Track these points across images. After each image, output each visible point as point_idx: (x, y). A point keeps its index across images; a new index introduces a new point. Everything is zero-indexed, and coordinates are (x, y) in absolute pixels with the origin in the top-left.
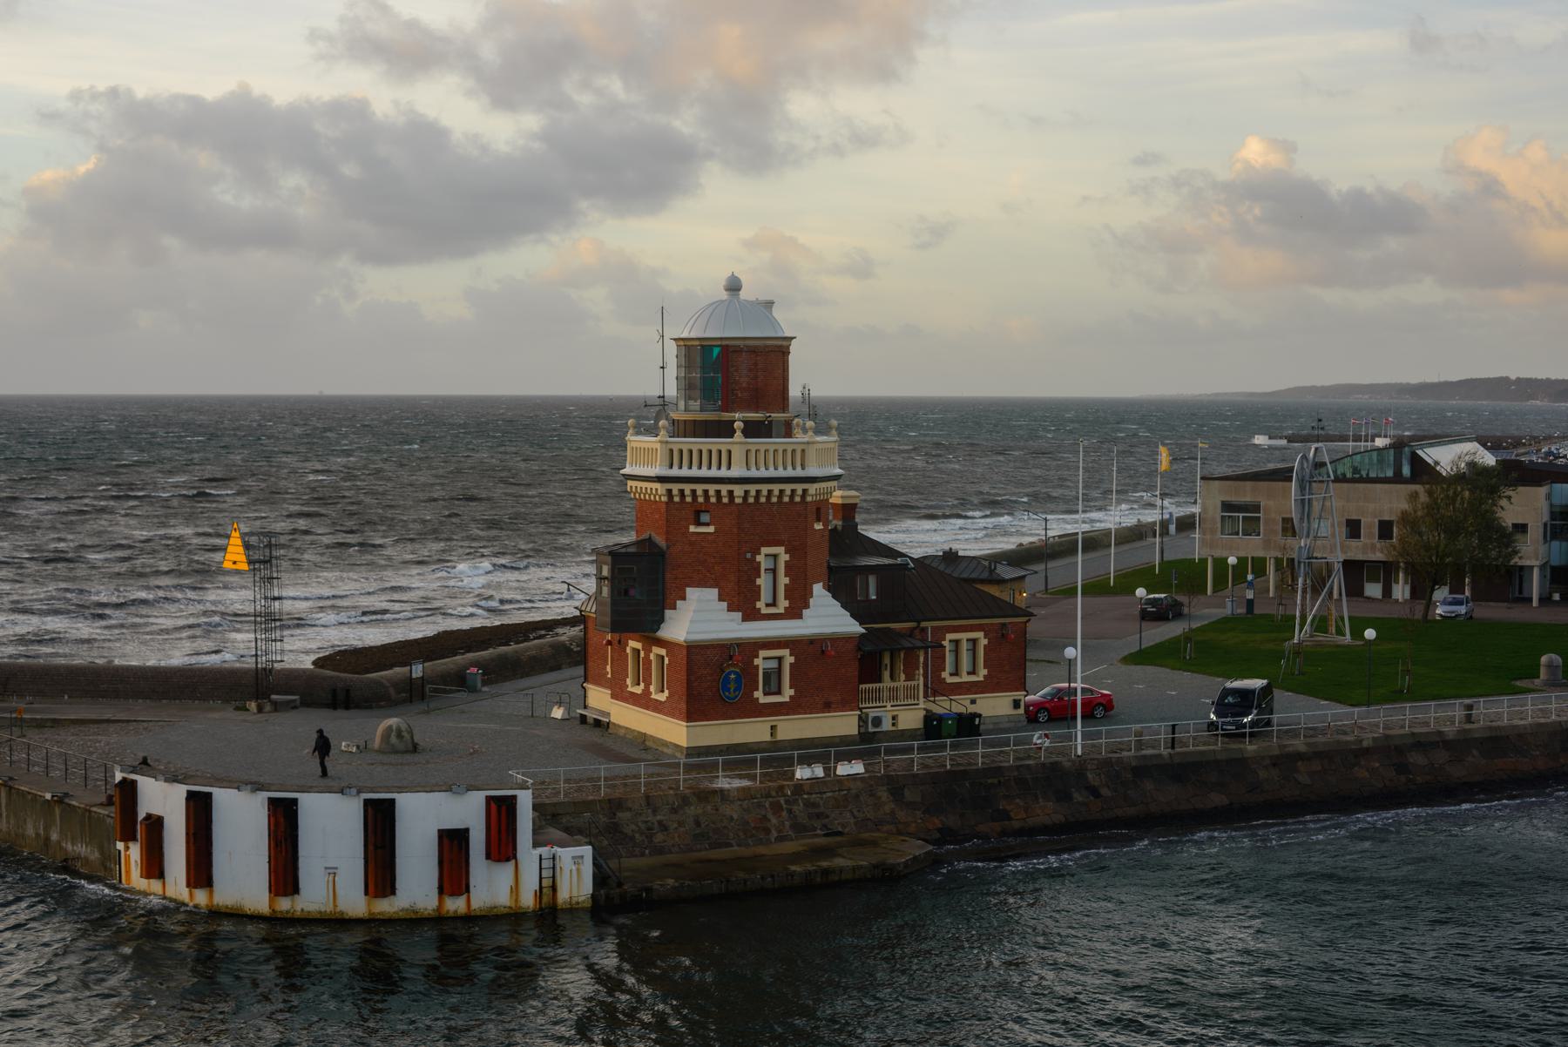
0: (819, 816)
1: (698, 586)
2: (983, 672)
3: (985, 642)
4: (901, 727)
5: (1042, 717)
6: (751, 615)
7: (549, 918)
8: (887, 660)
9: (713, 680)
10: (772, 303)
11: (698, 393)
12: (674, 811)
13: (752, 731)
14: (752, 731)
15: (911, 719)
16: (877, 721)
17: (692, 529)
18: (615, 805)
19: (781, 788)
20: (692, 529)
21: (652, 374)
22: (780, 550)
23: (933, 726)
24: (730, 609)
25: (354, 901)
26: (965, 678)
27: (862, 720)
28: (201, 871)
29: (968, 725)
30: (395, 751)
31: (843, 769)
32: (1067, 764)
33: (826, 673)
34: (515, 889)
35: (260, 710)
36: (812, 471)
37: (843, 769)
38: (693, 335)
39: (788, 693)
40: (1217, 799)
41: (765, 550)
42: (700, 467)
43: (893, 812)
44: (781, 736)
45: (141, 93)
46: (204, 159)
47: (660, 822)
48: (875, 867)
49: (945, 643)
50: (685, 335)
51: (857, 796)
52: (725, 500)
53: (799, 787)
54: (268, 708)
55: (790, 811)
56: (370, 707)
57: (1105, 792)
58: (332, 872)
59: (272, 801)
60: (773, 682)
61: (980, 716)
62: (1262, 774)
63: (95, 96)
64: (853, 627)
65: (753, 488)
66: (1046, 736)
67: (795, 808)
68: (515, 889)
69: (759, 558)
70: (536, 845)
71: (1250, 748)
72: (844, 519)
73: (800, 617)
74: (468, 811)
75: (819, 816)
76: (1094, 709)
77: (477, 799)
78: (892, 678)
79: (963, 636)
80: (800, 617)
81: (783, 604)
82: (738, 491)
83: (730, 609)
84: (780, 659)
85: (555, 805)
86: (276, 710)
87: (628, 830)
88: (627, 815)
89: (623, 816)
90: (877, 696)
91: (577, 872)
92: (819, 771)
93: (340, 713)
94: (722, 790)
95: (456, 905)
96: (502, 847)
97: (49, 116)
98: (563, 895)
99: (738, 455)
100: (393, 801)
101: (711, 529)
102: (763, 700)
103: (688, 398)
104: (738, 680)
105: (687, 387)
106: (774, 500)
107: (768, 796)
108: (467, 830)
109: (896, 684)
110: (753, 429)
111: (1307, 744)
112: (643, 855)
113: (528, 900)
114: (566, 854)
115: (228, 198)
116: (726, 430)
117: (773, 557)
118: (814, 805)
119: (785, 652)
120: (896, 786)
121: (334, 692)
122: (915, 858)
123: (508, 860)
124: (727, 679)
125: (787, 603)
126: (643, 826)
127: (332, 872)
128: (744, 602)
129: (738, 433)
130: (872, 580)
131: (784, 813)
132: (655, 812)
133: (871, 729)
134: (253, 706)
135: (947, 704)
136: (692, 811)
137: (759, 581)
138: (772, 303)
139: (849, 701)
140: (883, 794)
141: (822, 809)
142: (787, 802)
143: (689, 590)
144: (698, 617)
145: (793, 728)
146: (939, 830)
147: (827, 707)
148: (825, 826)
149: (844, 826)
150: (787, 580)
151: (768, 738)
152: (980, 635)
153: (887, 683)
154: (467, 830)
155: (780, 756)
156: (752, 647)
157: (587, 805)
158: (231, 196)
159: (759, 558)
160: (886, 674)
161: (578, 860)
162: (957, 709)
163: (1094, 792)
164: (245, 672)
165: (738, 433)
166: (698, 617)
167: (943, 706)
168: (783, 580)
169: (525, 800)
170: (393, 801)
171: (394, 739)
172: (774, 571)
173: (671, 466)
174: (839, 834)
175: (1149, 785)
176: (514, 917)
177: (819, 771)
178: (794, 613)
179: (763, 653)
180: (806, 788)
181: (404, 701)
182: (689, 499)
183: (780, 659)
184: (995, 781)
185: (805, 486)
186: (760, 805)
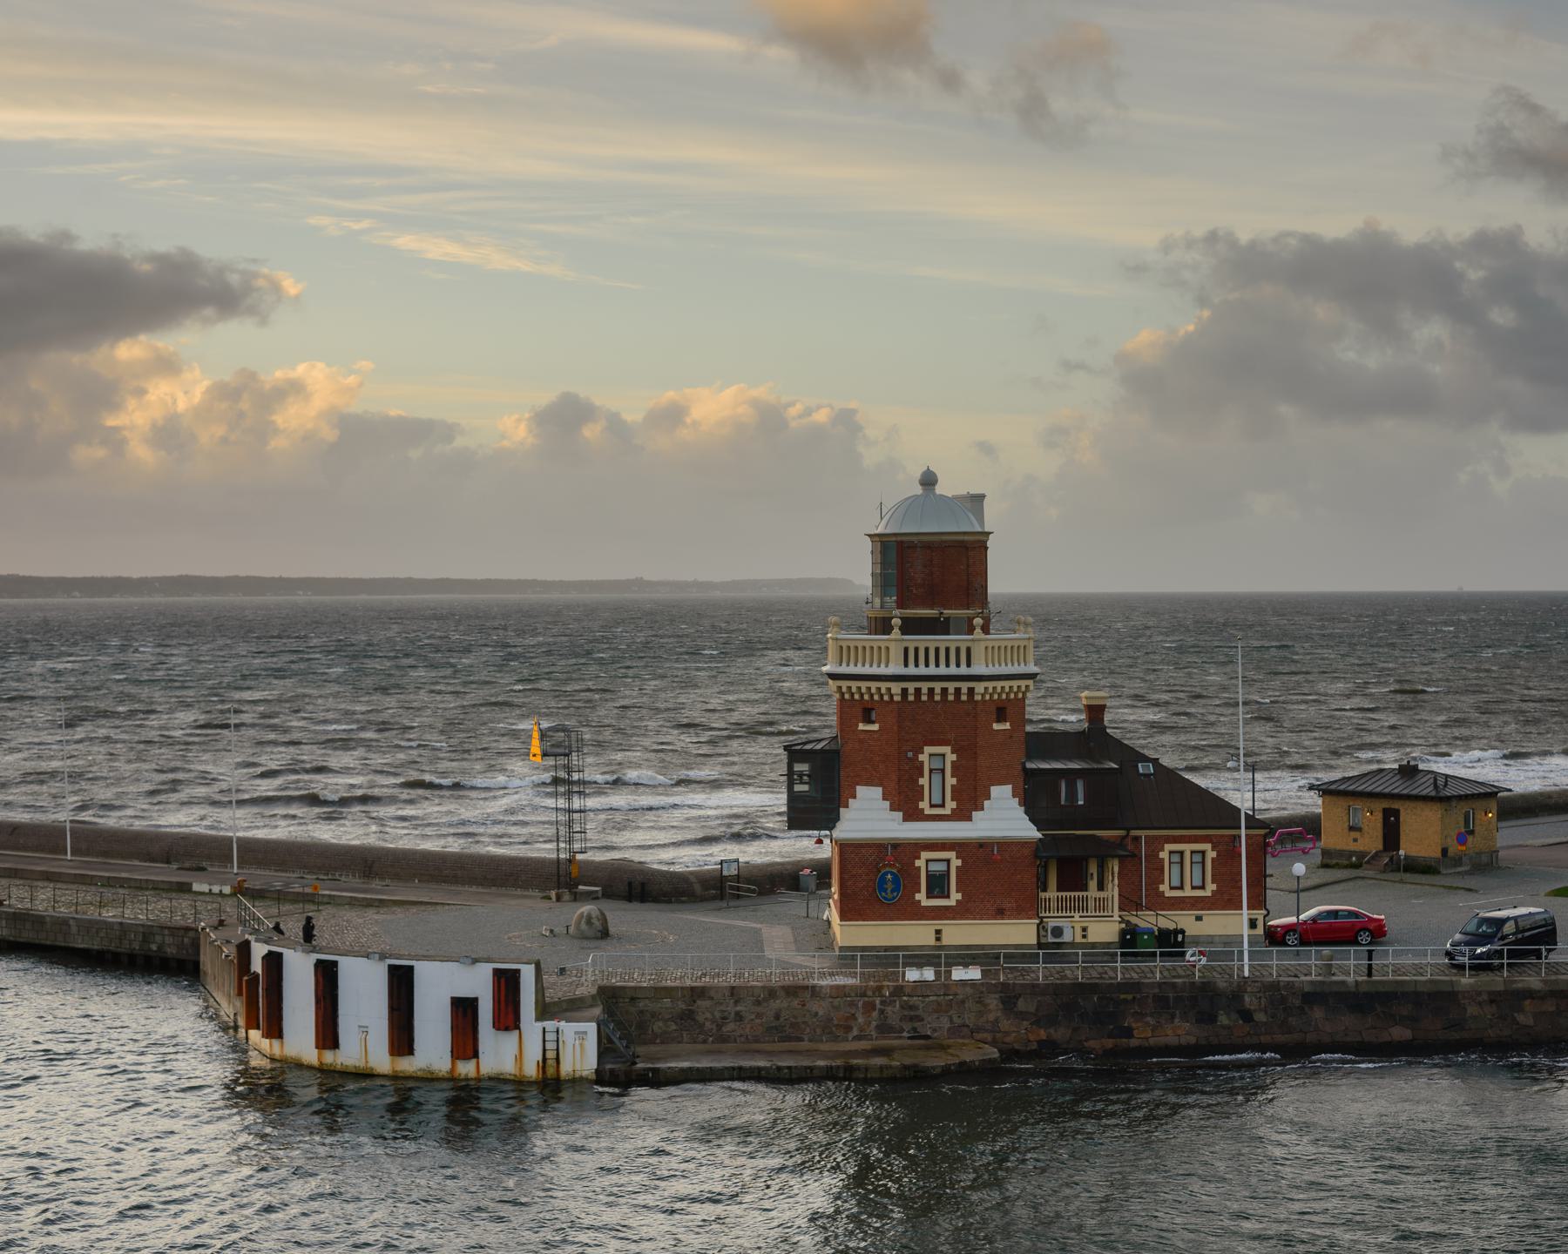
0: (911, 1019)
1: (867, 784)
2: (1211, 887)
3: (1214, 854)
4: (1091, 939)
5: (1291, 939)
6: (913, 815)
7: (551, 1087)
8: (1093, 869)
9: (876, 880)
10: (979, 499)
11: (894, 590)
12: (758, 1003)
13: (916, 934)
14: (916, 934)
15: (1105, 930)
16: (1058, 931)
17: (861, 727)
18: (697, 993)
19: (880, 988)
20: (861, 727)
21: (856, 573)
22: (946, 750)
23: (1130, 937)
24: (892, 809)
25: (380, 1059)
26: (1188, 892)
27: (1041, 927)
28: (328, 1034)
29: (1171, 941)
30: (587, 938)
31: (958, 974)
32: (1222, 984)
33: (991, 877)
34: (519, 1058)
35: (559, 899)
36: (979, 669)
37: (958, 974)
38: (888, 531)
39: (955, 897)
40: (1400, 1033)
41: (928, 750)
42: (937, 665)
43: (997, 1020)
44: (946, 941)
45: (1244, 237)
46: (1323, 312)
47: (737, 1013)
48: (905, 1067)
49: (1164, 855)
50: (880, 531)
51: (963, 1002)
52: (886, 698)
53: (899, 991)
54: (567, 897)
55: (882, 1012)
56: (669, 902)
57: (1260, 1017)
58: (365, 1030)
59: (392, 969)
60: (938, 885)
61: (1183, 932)
62: (1472, 1010)
63: (1190, 243)
64: (1030, 832)
65: (911, 686)
66: (1201, 953)
67: (889, 1009)
68: (519, 1058)
69: (923, 757)
70: (538, 1019)
71: (1466, 980)
72: (1091, 720)
73: (969, 819)
74: (478, 983)
75: (911, 1019)
76: (1357, 934)
77: (485, 972)
78: (1101, 887)
79: (1187, 848)
80: (969, 819)
81: (951, 805)
82: (896, 688)
83: (892, 809)
84: (948, 861)
85: (635, 988)
86: (575, 900)
87: (700, 1018)
88: (708, 1003)
89: (702, 1004)
90: (1082, 906)
91: (579, 1046)
92: (929, 974)
93: (636, 905)
94: (814, 987)
95: (466, 1069)
96: (507, 1019)
97: (1135, 269)
98: (566, 1068)
99: (896, 653)
100: (411, 968)
101: (875, 727)
102: (926, 902)
103: (884, 594)
104: (896, 880)
105: (883, 582)
106: (937, 698)
107: (864, 995)
108: (476, 999)
109: (1102, 895)
110: (910, 626)
111: (1545, 982)
112: (705, 1042)
113: (531, 1070)
114: (568, 1029)
115: (1351, 355)
116: (883, 626)
117: (937, 757)
118: (912, 1008)
119: (951, 855)
120: (1009, 996)
121: (630, 884)
122: (963, 1063)
123: (507, 1029)
124: (883, 879)
125: (954, 805)
126: (718, 1015)
127: (365, 1030)
128: (906, 803)
129: (896, 630)
130: (1080, 785)
131: (875, 1014)
132: (736, 1002)
133: (1051, 939)
134: (553, 894)
135: (1153, 920)
136: (776, 1004)
137: (921, 781)
138: (979, 499)
139: (1028, 907)
140: (993, 1002)
141: (920, 1012)
142: (882, 1003)
143: (859, 788)
144: (868, 816)
145: (960, 933)
146: (1039, 1042)
147: (1000, 913)
148: (915, 1029)
149: (935, 1030)
150: (921, 781)
151: (932, 942)
152: (1207, 847)
153: (1093, 892)
154: (476, 999)
155: (889, 958)
156: (906, 851)
157: (669, 991)
158: (1358, 354)
159: (921, 757)
160: (1093, 884)
161: (582, 1035)
162: (1165, 924)
163: (1247, 1016)
164: (551, 861)
165: (896, 630)
166: (868, 816)
167: (1148, 920)
168: (951, 781)
169: (528, 974)
170: (411, 968)
171: (583, 926)
172: (943, 771)
173: (906, 665)
174: (927, 1037)
175: (1318, 1013)
176: (519, 1084)
177: (929, 974)
178: (962, 815)
179: (925, 855)
180: (907, 991)
181: (714, 898)
182: (857, 697)
183: (948, 861)
184: (1130, 997)
185: (971, 684)
186: (852, 1004)
